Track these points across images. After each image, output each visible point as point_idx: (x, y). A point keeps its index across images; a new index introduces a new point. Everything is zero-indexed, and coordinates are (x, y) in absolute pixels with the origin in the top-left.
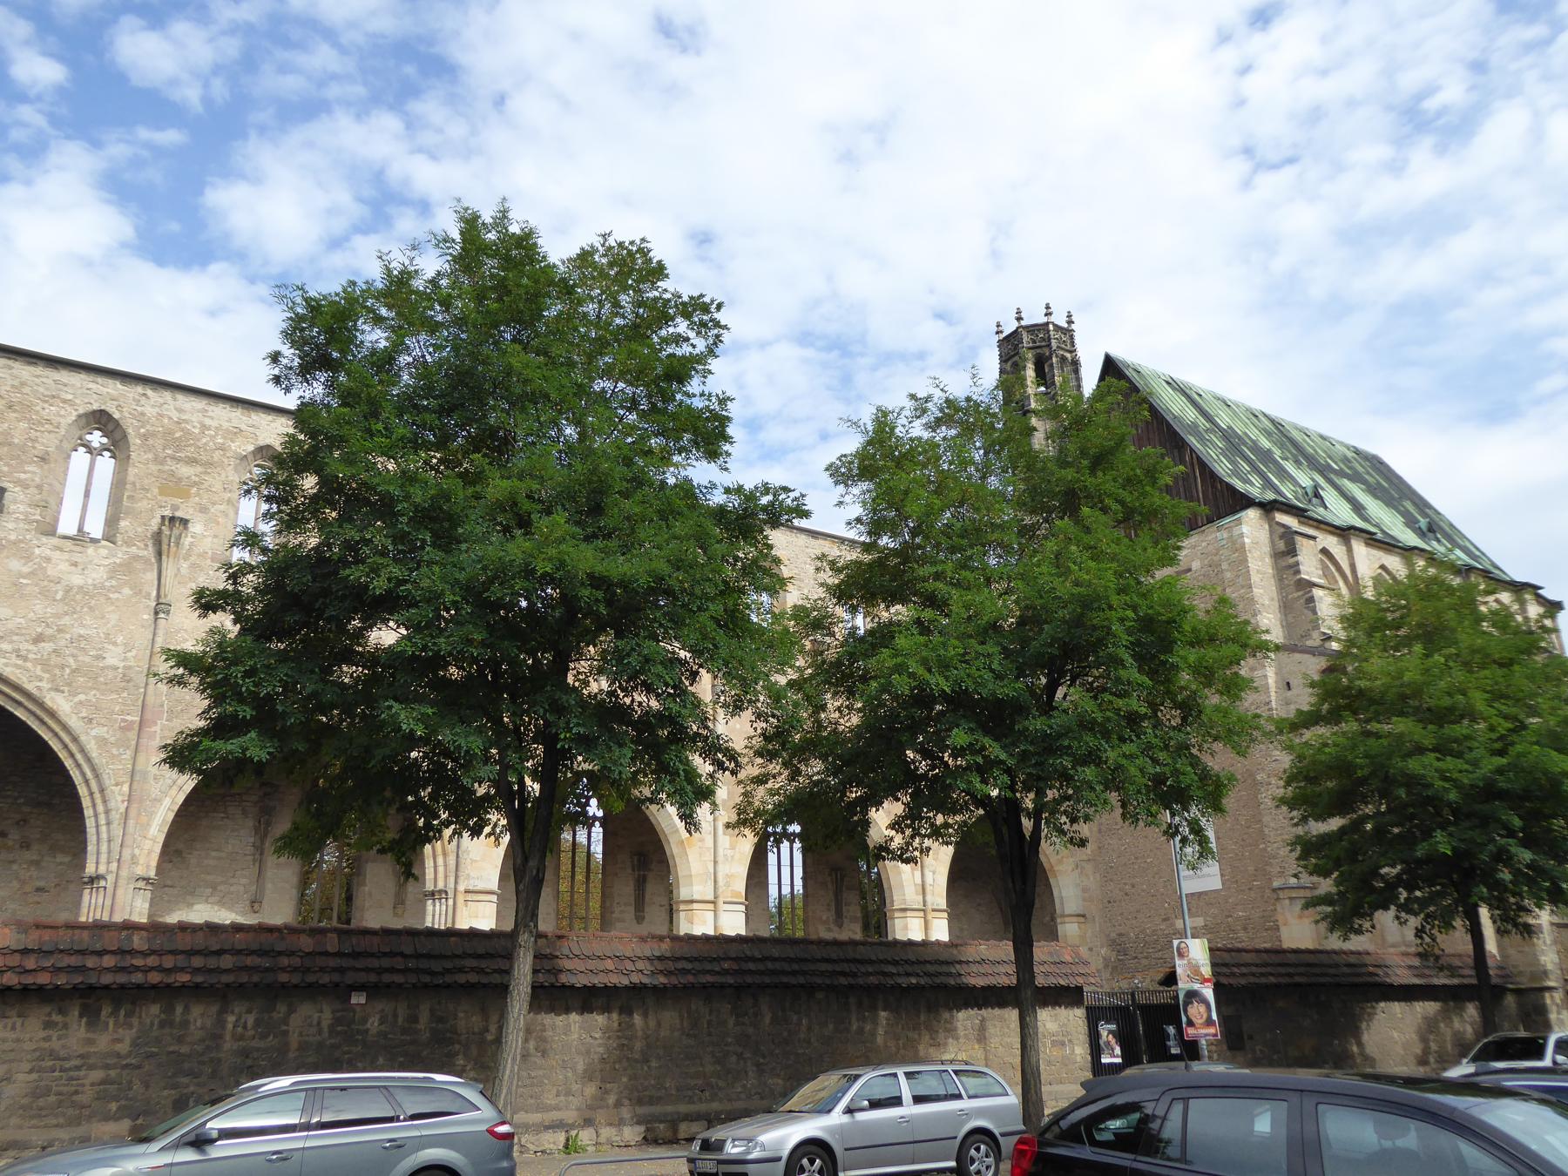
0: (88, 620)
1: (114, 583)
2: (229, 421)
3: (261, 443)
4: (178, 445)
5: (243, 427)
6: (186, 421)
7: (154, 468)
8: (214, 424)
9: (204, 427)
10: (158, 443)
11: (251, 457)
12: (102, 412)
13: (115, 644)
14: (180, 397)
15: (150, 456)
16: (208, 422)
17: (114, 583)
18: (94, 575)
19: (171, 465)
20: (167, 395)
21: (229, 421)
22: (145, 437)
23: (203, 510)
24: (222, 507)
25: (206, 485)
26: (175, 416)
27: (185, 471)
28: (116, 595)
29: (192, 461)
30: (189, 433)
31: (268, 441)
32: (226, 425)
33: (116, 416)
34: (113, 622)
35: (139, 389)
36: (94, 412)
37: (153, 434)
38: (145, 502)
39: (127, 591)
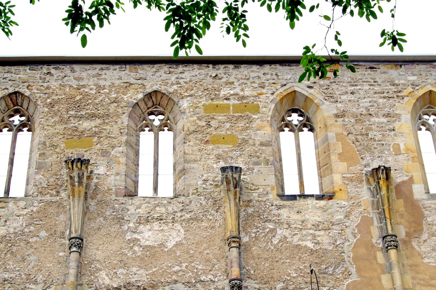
0: (11, 265)
1: (32, 228)
2: (120, 78)
3: (149, 90)
4: (78, 106)
5: (132, 81)
6: (84, 86)
7: (60, 128)
8: (108, 83)
9: (99, 88)
10: (63, 107)
11: (142, 105)
12: (16, 93)
13: (36, 283)
14: (76, 67)
15: (57, 119)
16: (102, 83)
17: (32, 228)
18: (15, 225)
19: (74, 123)
20: (67, 69)
21: (120, 78)
22: (51, 105)
23: (105, 153)
24: (121, 149)
25: (105, 133)
26: (74, 84)
27: (86, 125)
28: (34, 239)
29: (93, 116)
30: (87, 94)
31: (155, 88)
32: (117, 82)
33: (27, 93)
34: (33, 264)
35: (45, 69)
36: (10, 95)
37: (58, 102)
38: (55, 156)
39: (43, 234)
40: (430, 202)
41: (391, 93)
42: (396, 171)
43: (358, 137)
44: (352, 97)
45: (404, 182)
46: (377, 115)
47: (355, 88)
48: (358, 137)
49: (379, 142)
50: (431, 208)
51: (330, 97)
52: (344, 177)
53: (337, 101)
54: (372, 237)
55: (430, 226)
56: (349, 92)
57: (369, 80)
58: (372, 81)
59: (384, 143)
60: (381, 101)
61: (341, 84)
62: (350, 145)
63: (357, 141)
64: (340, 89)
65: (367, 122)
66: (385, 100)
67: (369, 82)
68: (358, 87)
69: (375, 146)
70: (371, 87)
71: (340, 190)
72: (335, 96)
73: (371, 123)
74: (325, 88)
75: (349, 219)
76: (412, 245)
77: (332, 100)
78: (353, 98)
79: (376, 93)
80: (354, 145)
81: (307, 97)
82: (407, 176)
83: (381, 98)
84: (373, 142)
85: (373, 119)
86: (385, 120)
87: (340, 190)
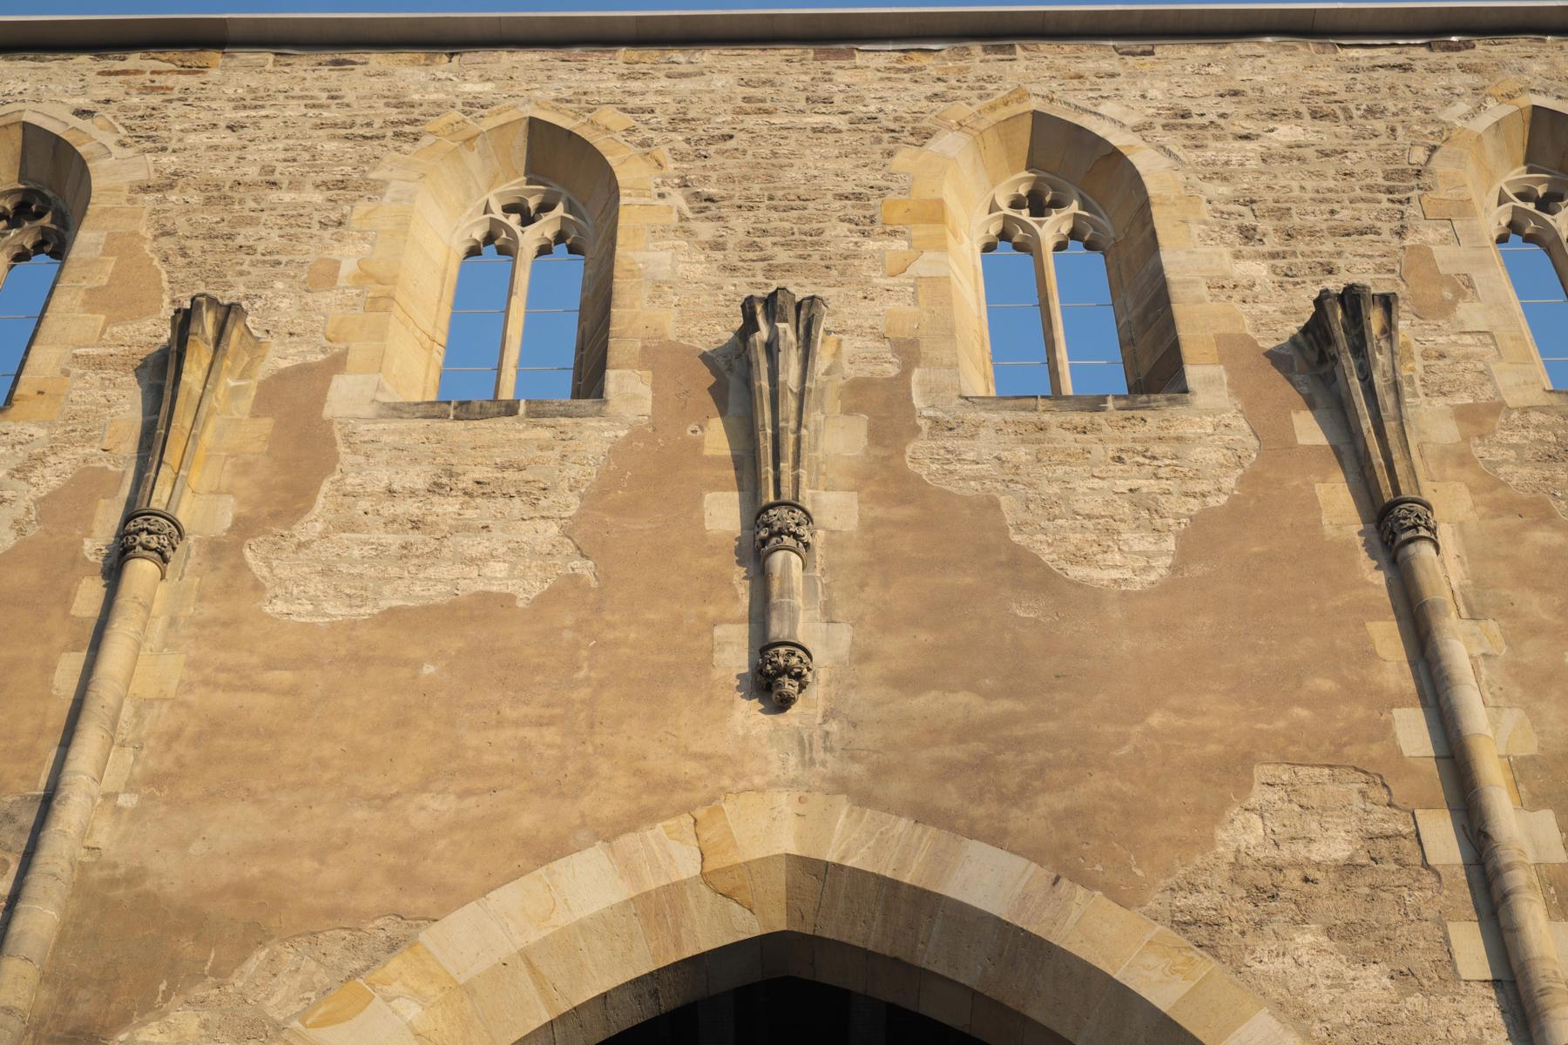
40: (381, 426)
41: (378, 123)
42: (295, 338)
43: (188, 243)
44: (231, 139)
45: (303, 370)
46: (295, 185)
47: (253, 113)
48: (188, 243)
49: (268, 258)
50: (378, 446)
51: (144, 134)
52: (76, 356)
53: (164, 149)
54: (89, 534)
55: (350, 500)
56: (223, 124)
57: (316, 93)
58: (325, 95)
59: (283, 259)
60: (332, 146)
61: (205, 104)
62: (150, 265)
63: (185, 255)
64: (193, 116)
65: (253, 205)
66: (350, 144)
67: (312, 98)
68: (263, 113)
69: (245, 267)
70: (311, 112)
71: (40, 393)
72: (165, 134)
73: (263, 206)
74: (140, 113)
75: (26, 479)
76: (242, 556)
77: (149, 145)
78: (230, 140)
79: (322, 126)
80: (163, 270)
81: (58, 137)
82: (324, 350)
83: (334, 137)
84: (242, 256)
85: (274, 195)
86: (318, 197)
87: (40, 393)
